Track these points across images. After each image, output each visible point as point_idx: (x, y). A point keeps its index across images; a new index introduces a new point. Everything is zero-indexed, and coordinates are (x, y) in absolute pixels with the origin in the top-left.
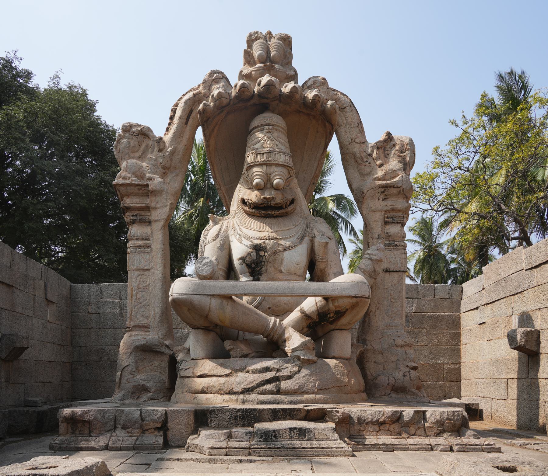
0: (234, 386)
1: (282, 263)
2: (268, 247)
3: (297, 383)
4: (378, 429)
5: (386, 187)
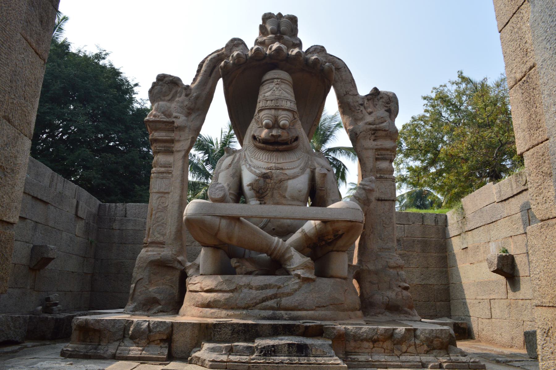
1: (286, 190)
3: (297, 300)
5: (376, 130)
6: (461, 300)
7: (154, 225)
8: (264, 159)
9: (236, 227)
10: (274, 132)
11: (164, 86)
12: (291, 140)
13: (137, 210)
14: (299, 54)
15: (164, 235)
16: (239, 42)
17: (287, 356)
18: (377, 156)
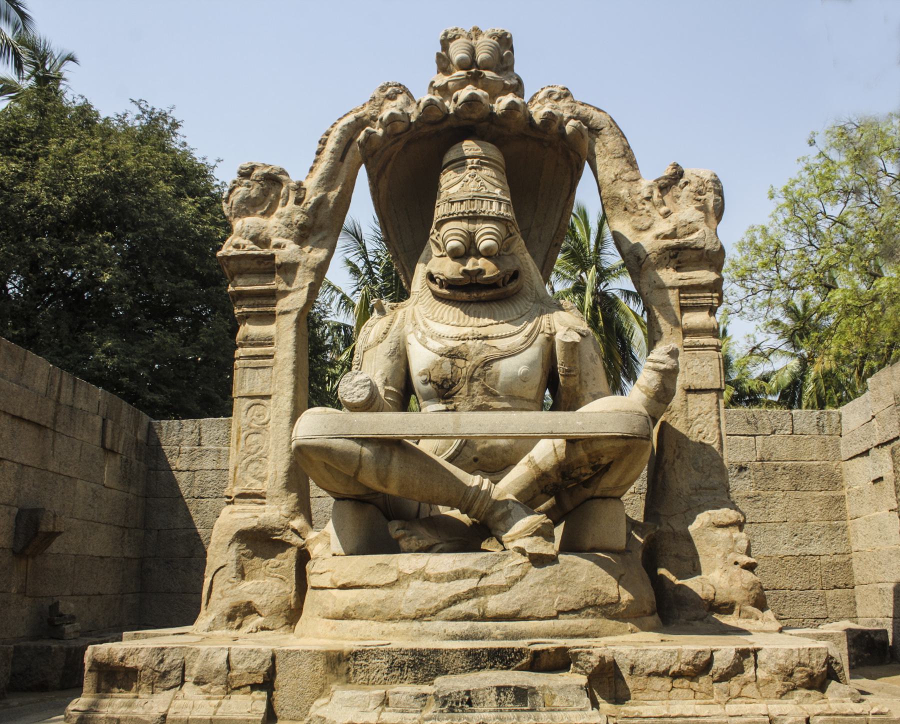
0: (402, 606)
1: (497, 378)
2: (472, 352)
3: (519, 600)
4: (670, 686)
5: (679, 249)
6: (875, 585)
7: (245, 461)
8: (451, 319)
9: (395, 460)
10: (470, 265)
11: (253, 186)
12: (504, 278)
13: (220, 431)
14: (512, 107)
15: (263, 479)
16: (397, 89)
17: (495, 711)
18: (682, 302)
